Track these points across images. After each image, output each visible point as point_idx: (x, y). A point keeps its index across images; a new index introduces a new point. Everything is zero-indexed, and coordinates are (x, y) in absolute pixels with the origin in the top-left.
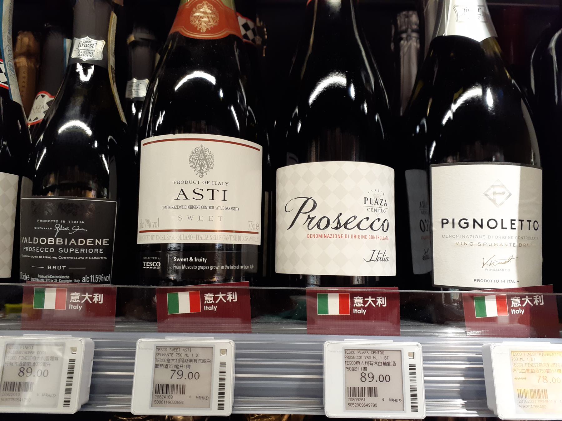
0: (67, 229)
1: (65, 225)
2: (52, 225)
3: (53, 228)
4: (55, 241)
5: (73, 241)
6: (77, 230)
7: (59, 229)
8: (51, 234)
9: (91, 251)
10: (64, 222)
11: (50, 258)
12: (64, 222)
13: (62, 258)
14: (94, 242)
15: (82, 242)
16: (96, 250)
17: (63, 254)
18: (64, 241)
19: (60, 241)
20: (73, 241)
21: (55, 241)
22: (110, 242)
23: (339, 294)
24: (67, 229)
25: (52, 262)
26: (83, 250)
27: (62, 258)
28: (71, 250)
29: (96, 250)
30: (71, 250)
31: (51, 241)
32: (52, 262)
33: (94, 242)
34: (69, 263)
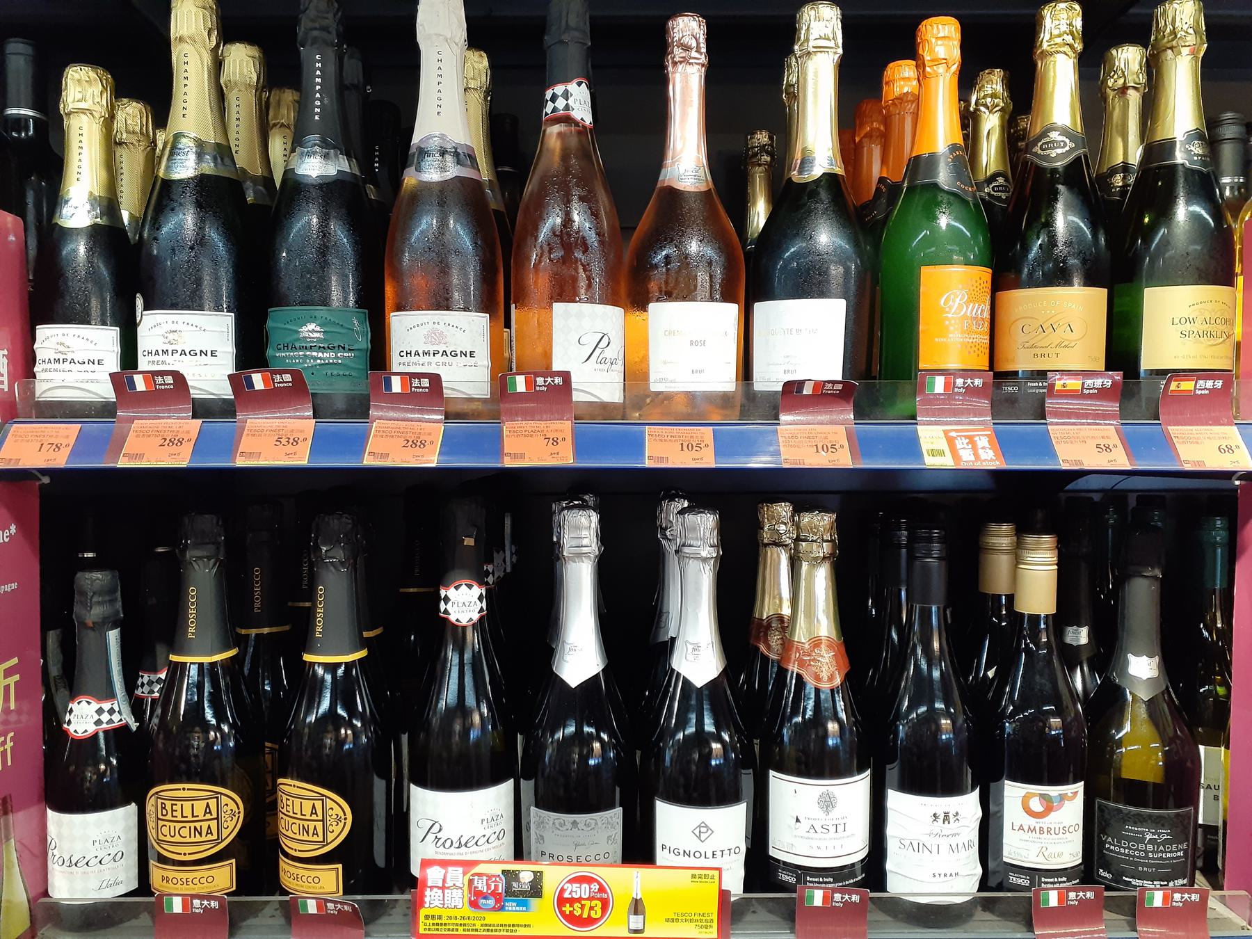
0: (1156, 837)
1: (1153, 834)
2: (1142, 833)
3: (1144, 835)
4: (1146, 847)
5: (1161, 848)
6: (1164, 837)
7: (1148, 837)
8: (1142, 840)
9: (1175, 855)
10: (1154, 831)
11: (1141, 860)
12: (1154, 831)
13: (1152, 862)
14: (1177, 847)
15: (1168, 848)
16: (1179, 854)
17: (1153, 859)
18: (1154, 848)
19: (1150, 847)
20: (1161, 848)
21: (1146, 847)
22: (1187, 845)
23: (1058, 892)
24: (1156, 837)
25: (1143, 865)
26: (1168, 855)
27: (1152, 862)
28: (1160, 855)
29: (1179, 854)
30: (1160, 855)
31: (1141, 846)
32: (1143, 865)
33: (1177, 847)
34: (1158, 866)
